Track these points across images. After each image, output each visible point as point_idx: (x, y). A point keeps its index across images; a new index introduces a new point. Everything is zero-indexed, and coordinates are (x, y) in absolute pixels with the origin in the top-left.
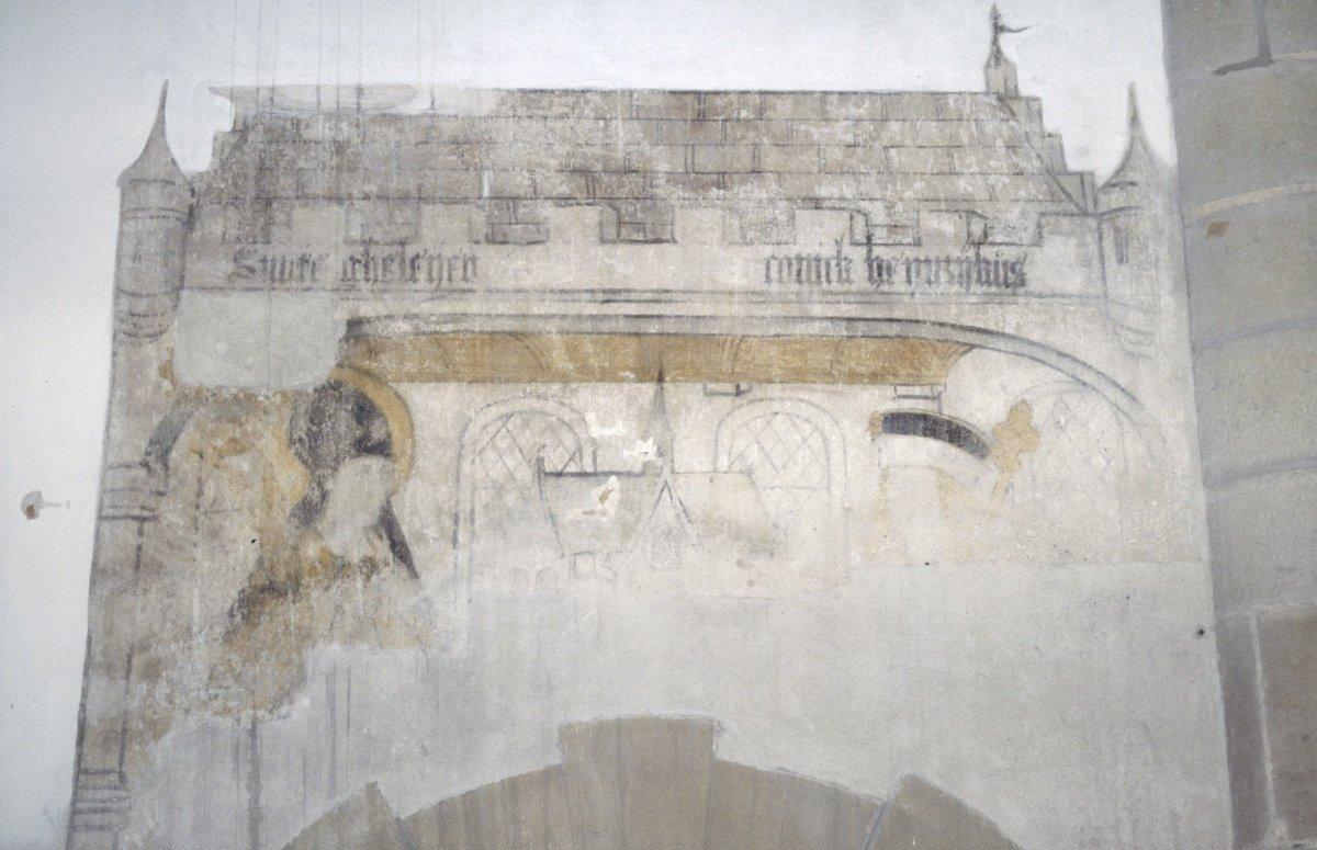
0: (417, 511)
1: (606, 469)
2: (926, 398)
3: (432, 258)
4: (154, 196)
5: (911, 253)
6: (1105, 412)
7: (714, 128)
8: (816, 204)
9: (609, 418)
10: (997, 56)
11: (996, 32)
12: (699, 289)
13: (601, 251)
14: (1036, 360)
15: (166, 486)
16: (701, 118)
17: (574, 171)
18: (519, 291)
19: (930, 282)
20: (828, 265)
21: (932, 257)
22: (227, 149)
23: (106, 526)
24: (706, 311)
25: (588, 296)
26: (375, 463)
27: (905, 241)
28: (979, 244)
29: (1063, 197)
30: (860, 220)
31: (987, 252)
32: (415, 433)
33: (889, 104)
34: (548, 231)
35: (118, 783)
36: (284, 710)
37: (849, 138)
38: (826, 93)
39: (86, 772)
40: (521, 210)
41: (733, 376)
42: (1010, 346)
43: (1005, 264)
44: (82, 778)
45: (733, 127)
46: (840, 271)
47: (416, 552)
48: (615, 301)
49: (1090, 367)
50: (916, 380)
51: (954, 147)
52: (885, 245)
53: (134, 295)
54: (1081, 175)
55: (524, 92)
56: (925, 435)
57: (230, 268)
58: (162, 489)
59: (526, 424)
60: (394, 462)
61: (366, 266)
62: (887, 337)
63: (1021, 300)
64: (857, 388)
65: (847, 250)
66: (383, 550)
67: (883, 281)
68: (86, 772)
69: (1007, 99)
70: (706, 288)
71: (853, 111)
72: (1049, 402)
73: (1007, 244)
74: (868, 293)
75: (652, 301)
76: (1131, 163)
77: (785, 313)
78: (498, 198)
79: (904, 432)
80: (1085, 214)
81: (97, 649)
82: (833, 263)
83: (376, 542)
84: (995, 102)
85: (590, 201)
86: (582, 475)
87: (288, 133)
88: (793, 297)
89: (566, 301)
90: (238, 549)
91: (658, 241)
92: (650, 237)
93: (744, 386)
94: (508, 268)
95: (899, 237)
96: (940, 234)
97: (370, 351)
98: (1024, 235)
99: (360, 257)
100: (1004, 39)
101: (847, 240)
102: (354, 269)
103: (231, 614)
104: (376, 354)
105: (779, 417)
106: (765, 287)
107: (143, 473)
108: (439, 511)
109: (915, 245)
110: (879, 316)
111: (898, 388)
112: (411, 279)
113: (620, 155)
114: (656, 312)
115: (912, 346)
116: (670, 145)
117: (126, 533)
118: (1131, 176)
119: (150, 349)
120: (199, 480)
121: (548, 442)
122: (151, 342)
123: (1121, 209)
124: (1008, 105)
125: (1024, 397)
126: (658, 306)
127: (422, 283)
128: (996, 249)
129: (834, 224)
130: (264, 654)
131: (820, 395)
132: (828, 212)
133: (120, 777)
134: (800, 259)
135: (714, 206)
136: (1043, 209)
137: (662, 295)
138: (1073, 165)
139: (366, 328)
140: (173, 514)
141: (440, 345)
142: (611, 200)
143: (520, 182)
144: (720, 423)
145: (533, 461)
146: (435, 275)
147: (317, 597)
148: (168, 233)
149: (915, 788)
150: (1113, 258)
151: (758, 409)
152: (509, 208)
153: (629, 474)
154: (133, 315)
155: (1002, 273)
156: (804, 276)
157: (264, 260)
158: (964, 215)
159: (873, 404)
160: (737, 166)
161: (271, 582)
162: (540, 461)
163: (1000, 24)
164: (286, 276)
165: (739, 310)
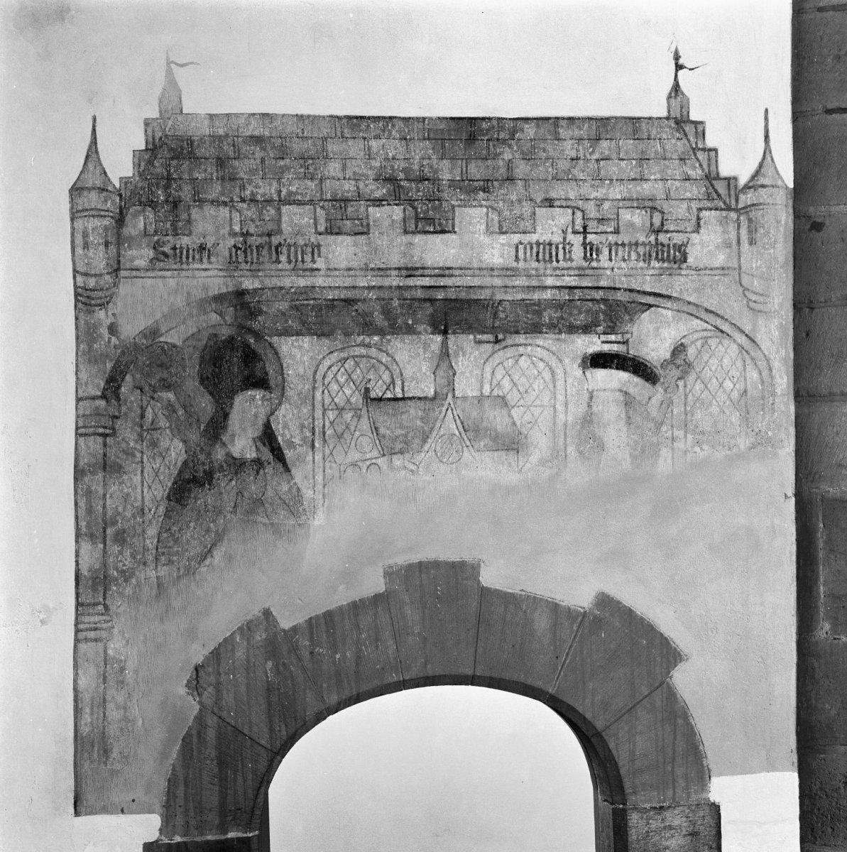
0: (288, 424)
1: (411, 395)
2: (619, 343)
3: (289, 246)
4: (93, 199)
5: (612, 238)
6: (734, 347)
7: (481, 144)
8: (549, 202)
9: (412, 360)
10: (676, 88)
11: (677, 71)
12: (471, 266)
13: (406, 239)
14: (692, 315)
15: (120, 412)
16: (472, 139)
17: (386, 180)
18: (350, 269)
19: (624, 260)
20: (557, 248)
21: (626, 242)
22: (143, 164)
23: (82, 440)
24: (476, 282)
25: (394, 273)
26: (258, 394)
27: (609, 230)
28: (658, 231)
29: (716, 197)
30: (579, 214)
31: (662, 238)
32: (284, 372)
33: (602, 127)
34: (368, 225)
35: (104, 612)
36: (207, 562)
37: (573, 154)
38: (558, 118)
39: (82, 605)
40: (350, 209)
41: (493, 330)
42: (675, 306)
43: (674, 245)
44: (80, 609)
45: (494, 146)
46: (565, 253)
47: (289, 454)
48: (414, 276)
49: (726, 320)
50: (611, 330)
51: (643, 159)
52: (596, 233)
53: (86, 274)
54: (728, 179)
55: (349, 118)
56: (617, 368)
57: (151, 254)
58: (117, 414)
59: (357, 364)
60: (271, 393)
61: (245, 252)
62: (595, 300)
63: (683, 272)
64: (574, 337)
65: (570, 237)
66: (267, 455)
67: (592, 260)
68: (82, 605)
69: (681, 122)
70: (475, 266)
71: (577, 133)
72: (699, 344)
73: (676, 232)
74: (583, 269)
75: (440, 276)
76: (762, 170)
77: (527, 284)
78: (336, 200)
79: (604, 367)
80: (729, 209)
81: (83, 524)
82: (561, 246)
83: (262, 448)
84: (673, 125)
85: (397, 202)
86: (396, 399)
87: (185, 152)
88: (534, 272)
89: (381, 276)
90: (171, 455)
91: (443, 232)
92: (438, 228)
93: (500, 336)
94: (342, 251)
95: (605, 227)
96: (631, 225)
97: (251, 314)
98: (687, 224)
99: (240, 246)
100: (681, 73)
101: (570, 230)
102: (236, 254)
103: (169, 498)
104: (256, 316)
105: (523, 358)
106: (514, 264)
107: (102, 403)
108: (302, 426)
109: (615, 233)
110: (590, 285)
111: (601, 336)
112: (276, 262)
113: (416, 167)
114: (442, 284)
115: (611, 306)
116: (452, 159)
117: (95, 444)
118: (762, 181)
119: (101, 314)
120: (142, 407)
121: (372, 377)
122: (101, 309)
123: (754, 205)
124: (682, 128)
125: (683, 341)
126: (443, 279)
127: (284, 264)
128: (668, 235)
129: (562, 217)
130: (192, 525)
131: (550, 342)
132: (558, 209)
133: (104, 607)
134: (538, 244)
135: (481, 206)
136: (701, 205)
137: (445, 271)
138: (725, 170)
139: (247, 298)
140: (127, 432)
141: (298, 309)
142: (411, 202)
143: (349, 187)
144: (485, 363)
145: (363, 391)
146: (292, 258)
147: (227, 487)
148: (106, 229)
149: (605, 601)
150: (746, 241)
151: (510, 352)
152: (341, 208)
153: (426, 398)
154: (86, 290)
155: (672, 251)
156: (541, 256)
157: (174, 248)
158: (649, 210)
159: (584, 347)
160: (497, 175)
161: (194, 477)
162: (367, 390)
163: (681, 62)
164: (191, 260)
165: (498, 282)
